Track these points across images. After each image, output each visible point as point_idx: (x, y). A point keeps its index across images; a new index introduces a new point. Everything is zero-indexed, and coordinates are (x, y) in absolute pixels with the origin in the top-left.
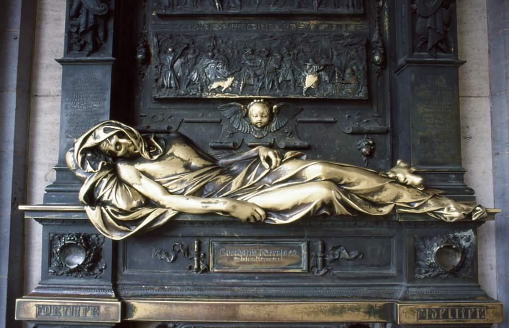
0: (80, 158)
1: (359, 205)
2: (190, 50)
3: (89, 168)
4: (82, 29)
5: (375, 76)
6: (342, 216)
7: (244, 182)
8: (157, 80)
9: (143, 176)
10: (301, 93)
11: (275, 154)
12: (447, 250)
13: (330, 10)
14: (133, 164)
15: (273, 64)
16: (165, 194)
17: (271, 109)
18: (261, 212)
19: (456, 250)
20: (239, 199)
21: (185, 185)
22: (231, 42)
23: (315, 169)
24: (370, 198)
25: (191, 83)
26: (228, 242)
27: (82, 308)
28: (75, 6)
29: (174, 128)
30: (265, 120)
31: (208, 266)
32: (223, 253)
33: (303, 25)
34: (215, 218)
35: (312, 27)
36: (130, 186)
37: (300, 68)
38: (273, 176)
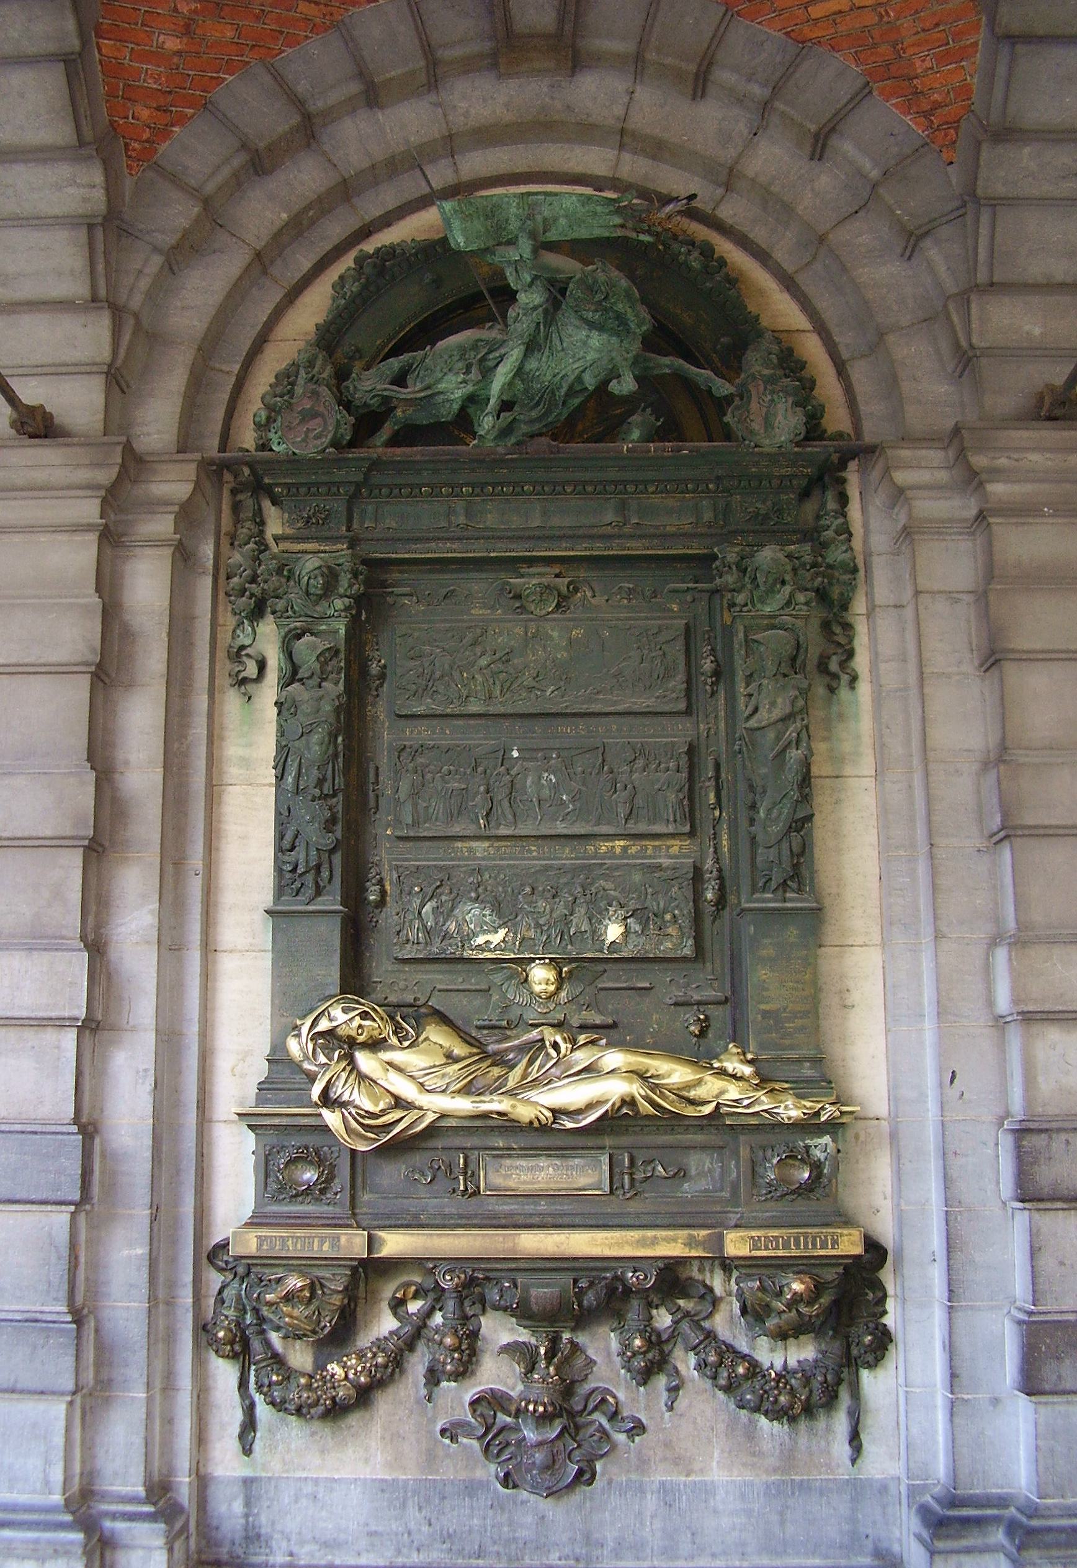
0: (310, 1046)
2: (446, 888)
3: (322, 1059)
7: (524, 1076)
10: (602, 951)
11: (564, 1039)
12: (791, 1162)
13: (642, 828)
15: (561, 910)
16: (421, 1092)
17: (560, 973)
18: (549, 1114)
20: (519, 1097)
22: (502, 876)
25: (446, 936)
28: (289, 837)
30: (552, 988)
31: (478, 1188)
33: (604, 847)
34: (490, 1123)
36: (375, 1082)
37: (600, 913)
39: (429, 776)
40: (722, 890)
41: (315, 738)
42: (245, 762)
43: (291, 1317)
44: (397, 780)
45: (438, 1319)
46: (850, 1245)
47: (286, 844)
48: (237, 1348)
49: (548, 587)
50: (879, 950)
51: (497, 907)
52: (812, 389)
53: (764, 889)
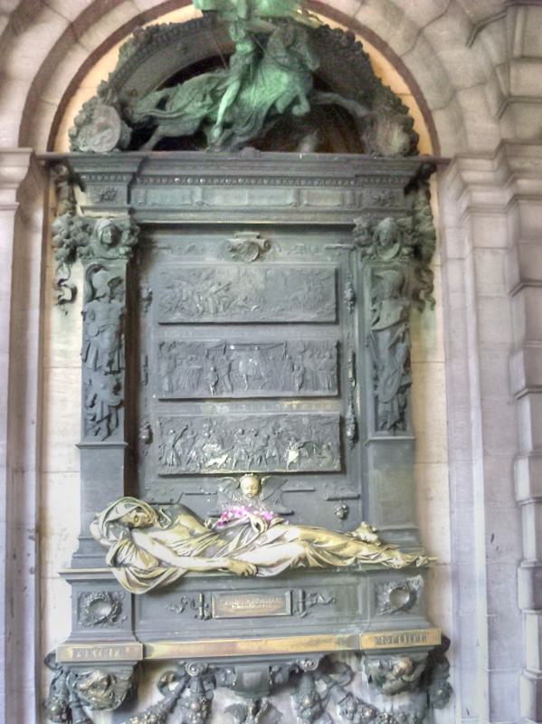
1: (328, 559)
3: (112, 537)
4: (97, 419)
5: (348, 448)
6: (315, 568)
7: (238, 545)
8: (160, 459)
9: (156, 543)
10: (285, 468)
13: (309, 393)
14: (146, 533)
15: (261, 443)
17: (260, 481)
18: (254, 568)
19: (406, 591)
21: (191, 548)
23: (293, 531)
24: (337, 553)
26: (228, 592)
27: (111, 650)
29: (175, 501)
32: (223, 603)
33: (286, 404)
35: (294, 407)
38: (262, 539)
39: (179, 361)
40: (356, 430)
41: (107, 334)
42: (64, 353)
43: (96, 697)
44: (158, 364)
45: (187, 693)
46: (433, 640)
47: (89, 403)
48: (64, 717)
49: (253, 244)
50: (446, 465)
51: (222, 442)
52: (412, 125)
53: (382, 428)
